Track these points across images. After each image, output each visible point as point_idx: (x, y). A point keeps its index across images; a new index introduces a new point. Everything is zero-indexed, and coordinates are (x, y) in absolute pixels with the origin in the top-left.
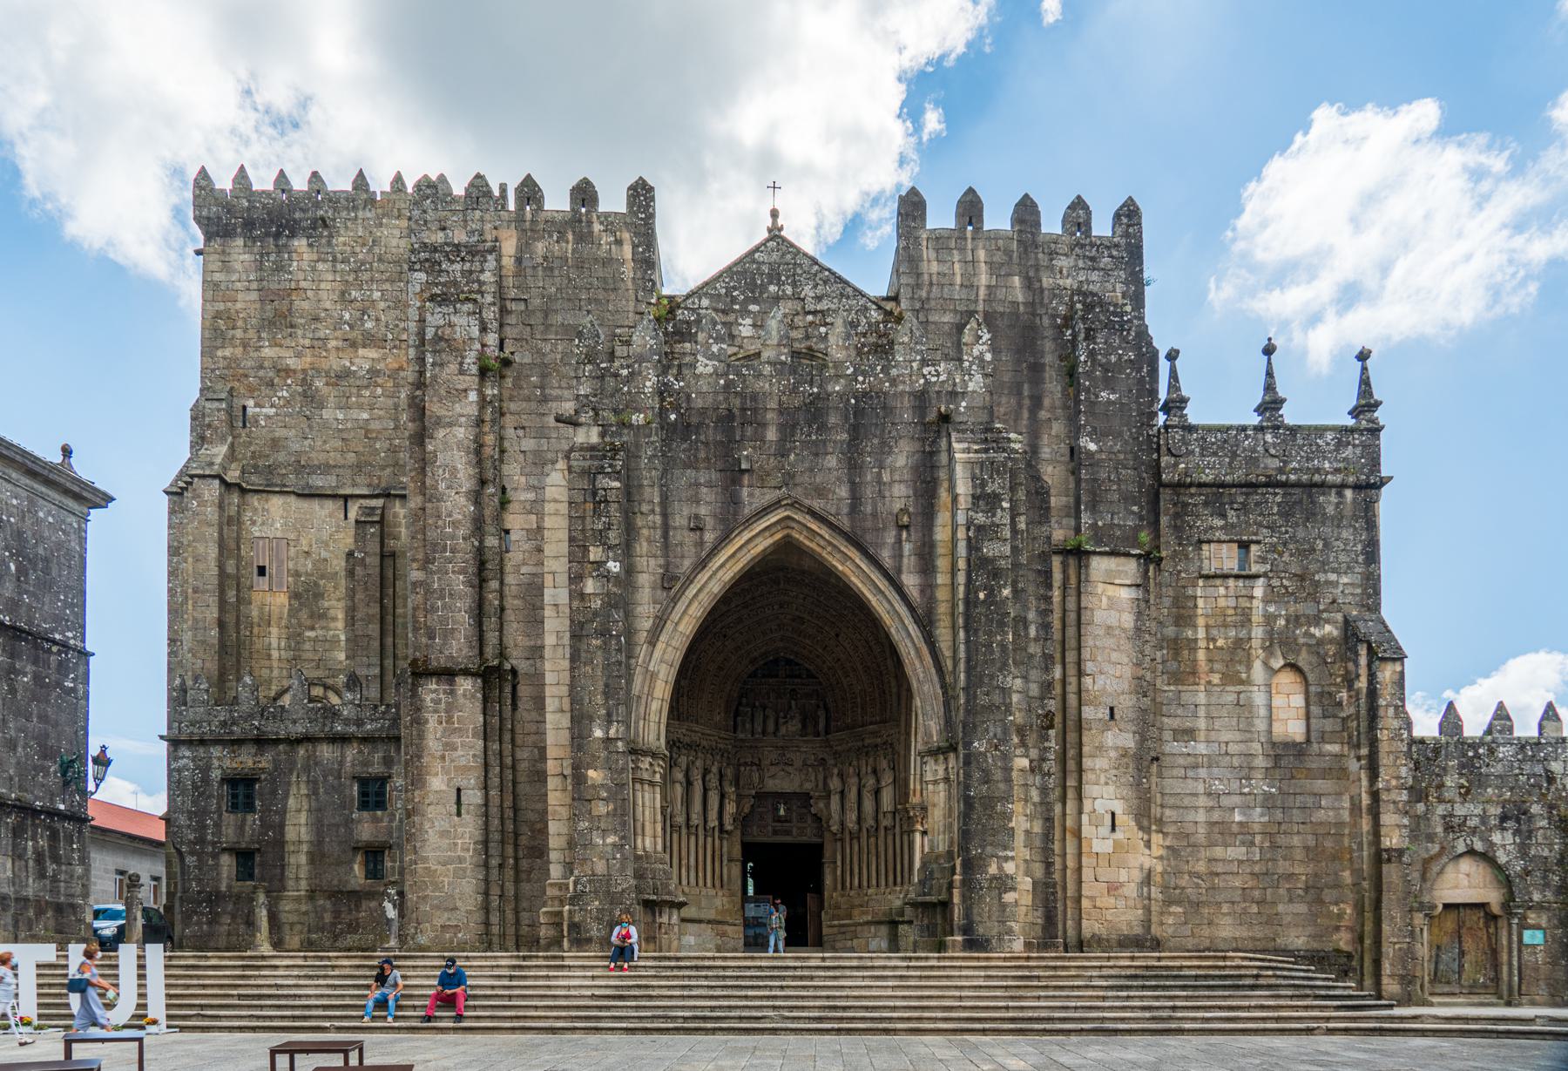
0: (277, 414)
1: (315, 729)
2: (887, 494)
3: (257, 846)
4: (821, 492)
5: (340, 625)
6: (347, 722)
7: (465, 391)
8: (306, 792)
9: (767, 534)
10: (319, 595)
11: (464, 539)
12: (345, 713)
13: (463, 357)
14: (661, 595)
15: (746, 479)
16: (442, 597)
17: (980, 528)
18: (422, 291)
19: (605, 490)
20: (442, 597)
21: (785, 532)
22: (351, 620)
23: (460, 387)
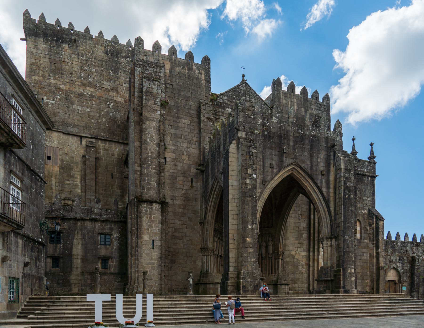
0: (55, 103)
1: (84, 216)
2: (319, 165)
3: (62, 256)
4: (303, 162)
5: (79, 180)
6: (96, 214)
7: (156, 110)
8: (81, 238)
9: (287, 172)
10: (71, 169)
11: (155, 158)
12: (96, 211)
13: (156, 99)
14: (262, 185)
15: (285, 155)
16: (147, 177)
17: (347, 178)
18: (140, 74)
19: (252, 152)
20: (147, 177)
21: (292, 172)
22: (84, 179)
23: (154, 108)
